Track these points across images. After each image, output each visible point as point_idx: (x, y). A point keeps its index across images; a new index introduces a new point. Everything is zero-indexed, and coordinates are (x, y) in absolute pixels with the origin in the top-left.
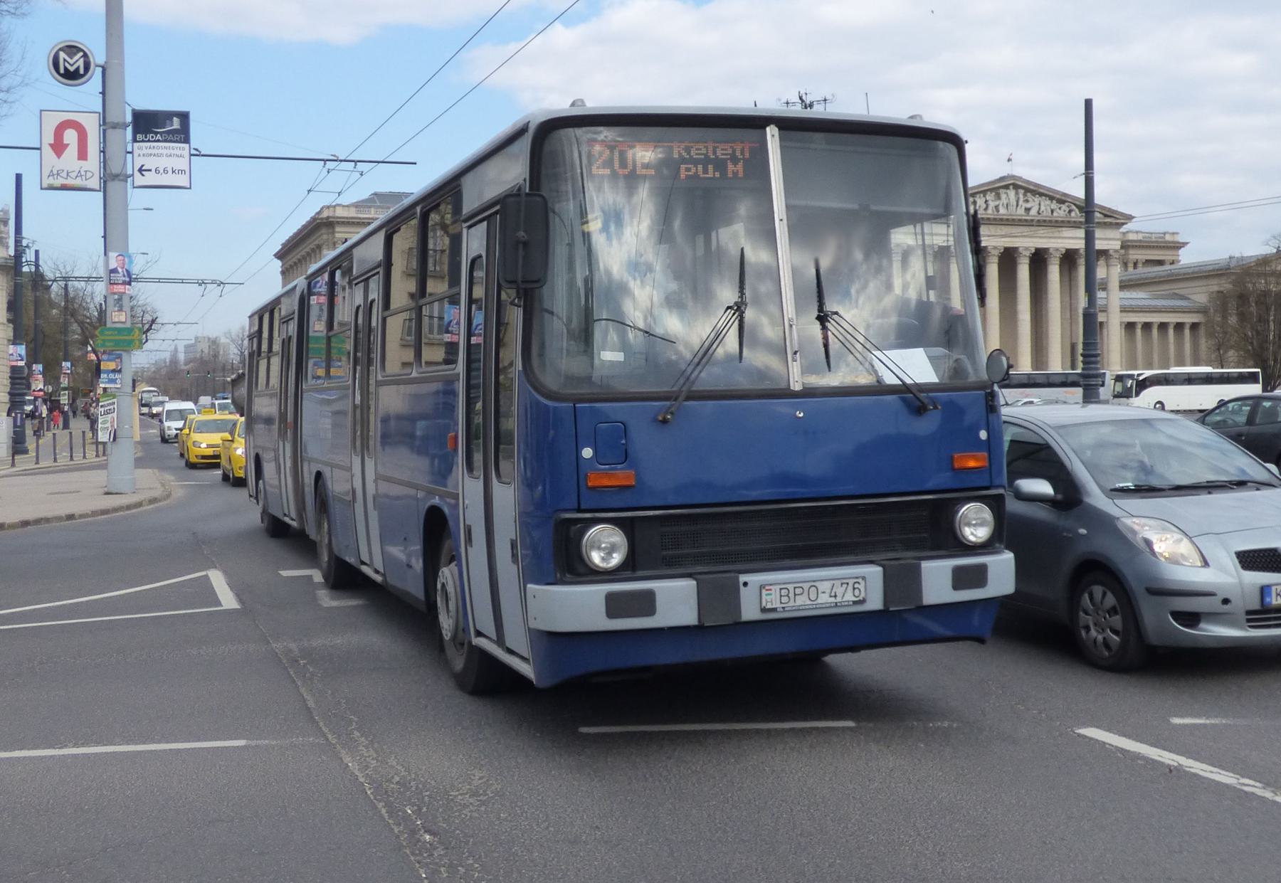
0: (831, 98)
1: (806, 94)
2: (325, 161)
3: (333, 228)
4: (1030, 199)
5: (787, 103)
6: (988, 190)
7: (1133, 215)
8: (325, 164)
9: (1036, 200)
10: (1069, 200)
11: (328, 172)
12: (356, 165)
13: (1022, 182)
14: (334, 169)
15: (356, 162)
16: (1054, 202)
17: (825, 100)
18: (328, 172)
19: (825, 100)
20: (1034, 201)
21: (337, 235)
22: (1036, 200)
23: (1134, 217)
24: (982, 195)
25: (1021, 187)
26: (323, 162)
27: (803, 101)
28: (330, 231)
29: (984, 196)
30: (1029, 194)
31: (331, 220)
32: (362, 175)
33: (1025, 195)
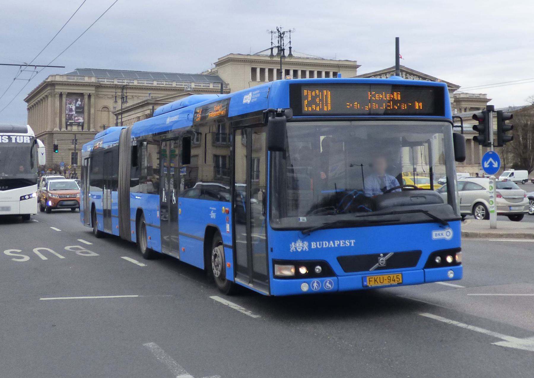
0: (293, 30)
1: (281, 28)
2: (21, 66)
3: (55, 87)
4: (408, 77)
5: (272, 32)
6: (387, 72)
7: (460, 86)
8: (21, 67)
9: (411, 77)
10: (428, 78)
11: (21, 72)
12: (36, 68)
13: (405, 69)
14: (23, 70)
15: (36, 66)
16: (421, 79)
17: (290, 31)
18: (21, 72)
19: (290, 31)
20: (410, 78)
21: (56, 90)
22: (411, 77)
23: (460, 87)
24: (384, 75)
25: (403, 71)
26: (20, 66)
27: (279, 31)
28: (53, 88)
29: (386, 75)
30: (408, 75)
31: (53, 82)
32: (37, 73)
33: (406, 75)
